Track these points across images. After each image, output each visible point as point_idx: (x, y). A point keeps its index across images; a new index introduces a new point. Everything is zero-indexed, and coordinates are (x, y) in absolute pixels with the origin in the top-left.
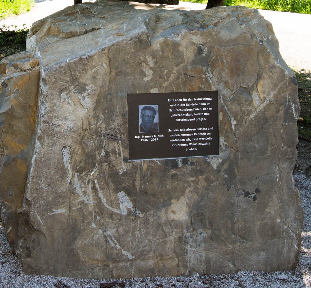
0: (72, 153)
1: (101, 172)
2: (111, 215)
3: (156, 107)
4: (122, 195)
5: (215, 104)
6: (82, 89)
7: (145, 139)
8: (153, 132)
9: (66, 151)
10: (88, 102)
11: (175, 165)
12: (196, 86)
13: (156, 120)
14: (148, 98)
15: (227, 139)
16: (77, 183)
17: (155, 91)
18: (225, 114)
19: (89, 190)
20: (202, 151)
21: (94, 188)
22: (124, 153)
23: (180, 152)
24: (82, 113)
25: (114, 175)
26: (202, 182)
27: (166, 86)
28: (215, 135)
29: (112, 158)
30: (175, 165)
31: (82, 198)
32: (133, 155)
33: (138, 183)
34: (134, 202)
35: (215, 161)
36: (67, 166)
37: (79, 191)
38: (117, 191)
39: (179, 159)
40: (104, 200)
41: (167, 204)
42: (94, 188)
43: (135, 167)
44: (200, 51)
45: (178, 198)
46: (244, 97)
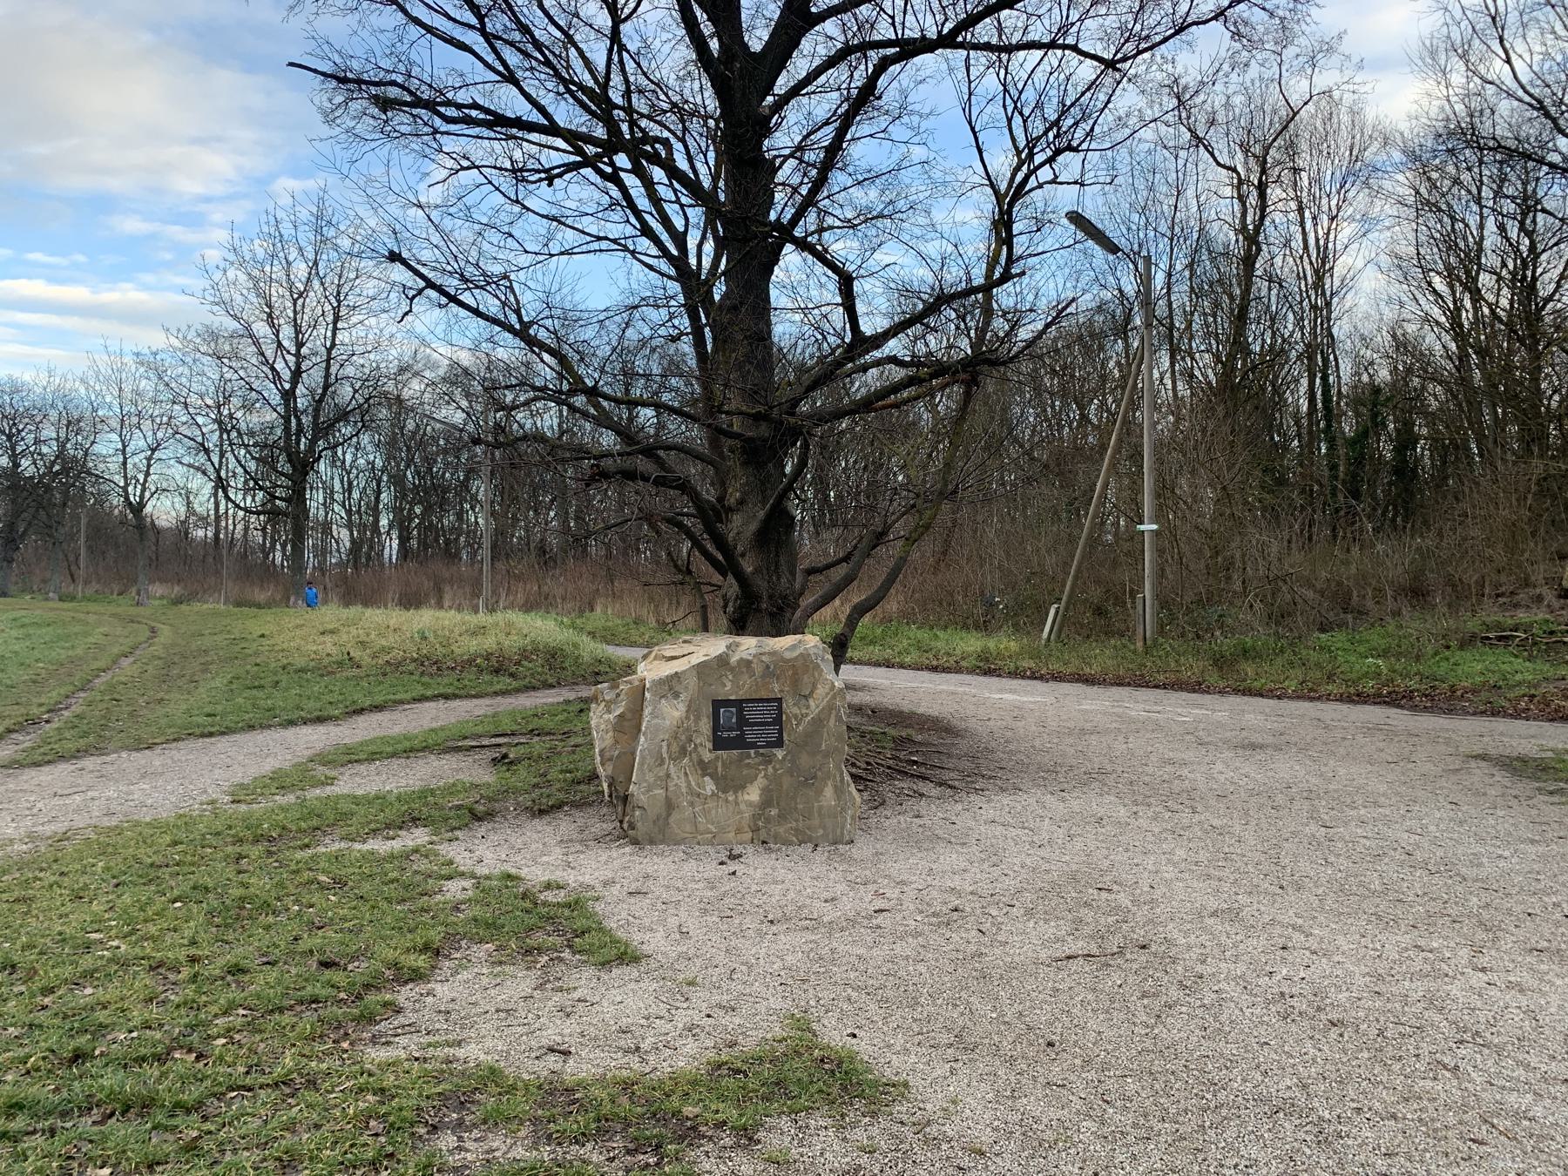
0: (668, 746)
1: (691, 760)
2: (699, 795)
3: (734, 710)
4: (707, 779)
5: (780, 708)
6: (676, 695)
7: (725, 735)
8: (731, 729)
9: (665, 744)
10: (682, 707)
11: (749, 756)
12: (764, 694)
13: (734, 720)
14: (727, 703)
15: (789, 735)
16: (672, 770)
17: (733, 698)
18: (787, 716)
19: (682, 775)
20: (770, 745)
21: (686, 774)
22: (710, 745)
23: (753, 746)
24: (677, 714)
25: (701, 762)
26: (770, 769)
27: (742, 695)
28: (781, 732)
29: (699, 749)
30: (749, 756)
31: (676, 781)
32: (716, 746)
33: (720, 769)
34: (716, 784)
35: (780, 754)
36: (665, 755)
37: (673, 775)
38: (704, 775)
39: (752, 751)
40: (693, 783)
41: (741, 787)
42: (686, 774)
43: (717, 758)
44: (768, 667)
45: (751, 783)
46: (804, 701)
